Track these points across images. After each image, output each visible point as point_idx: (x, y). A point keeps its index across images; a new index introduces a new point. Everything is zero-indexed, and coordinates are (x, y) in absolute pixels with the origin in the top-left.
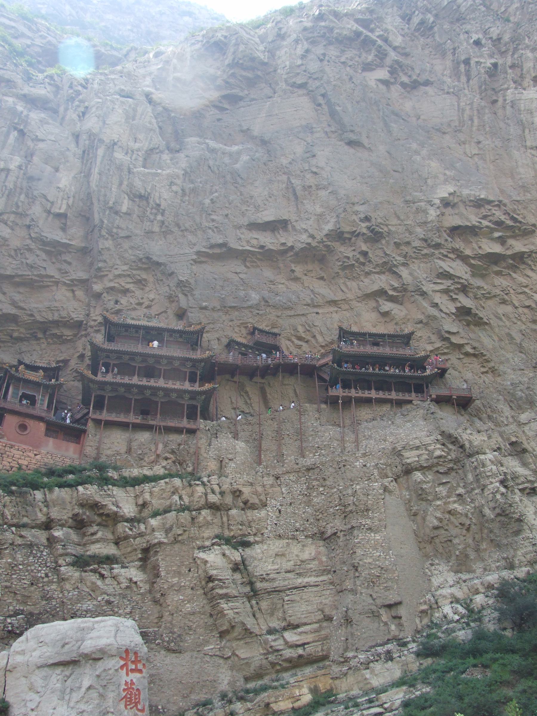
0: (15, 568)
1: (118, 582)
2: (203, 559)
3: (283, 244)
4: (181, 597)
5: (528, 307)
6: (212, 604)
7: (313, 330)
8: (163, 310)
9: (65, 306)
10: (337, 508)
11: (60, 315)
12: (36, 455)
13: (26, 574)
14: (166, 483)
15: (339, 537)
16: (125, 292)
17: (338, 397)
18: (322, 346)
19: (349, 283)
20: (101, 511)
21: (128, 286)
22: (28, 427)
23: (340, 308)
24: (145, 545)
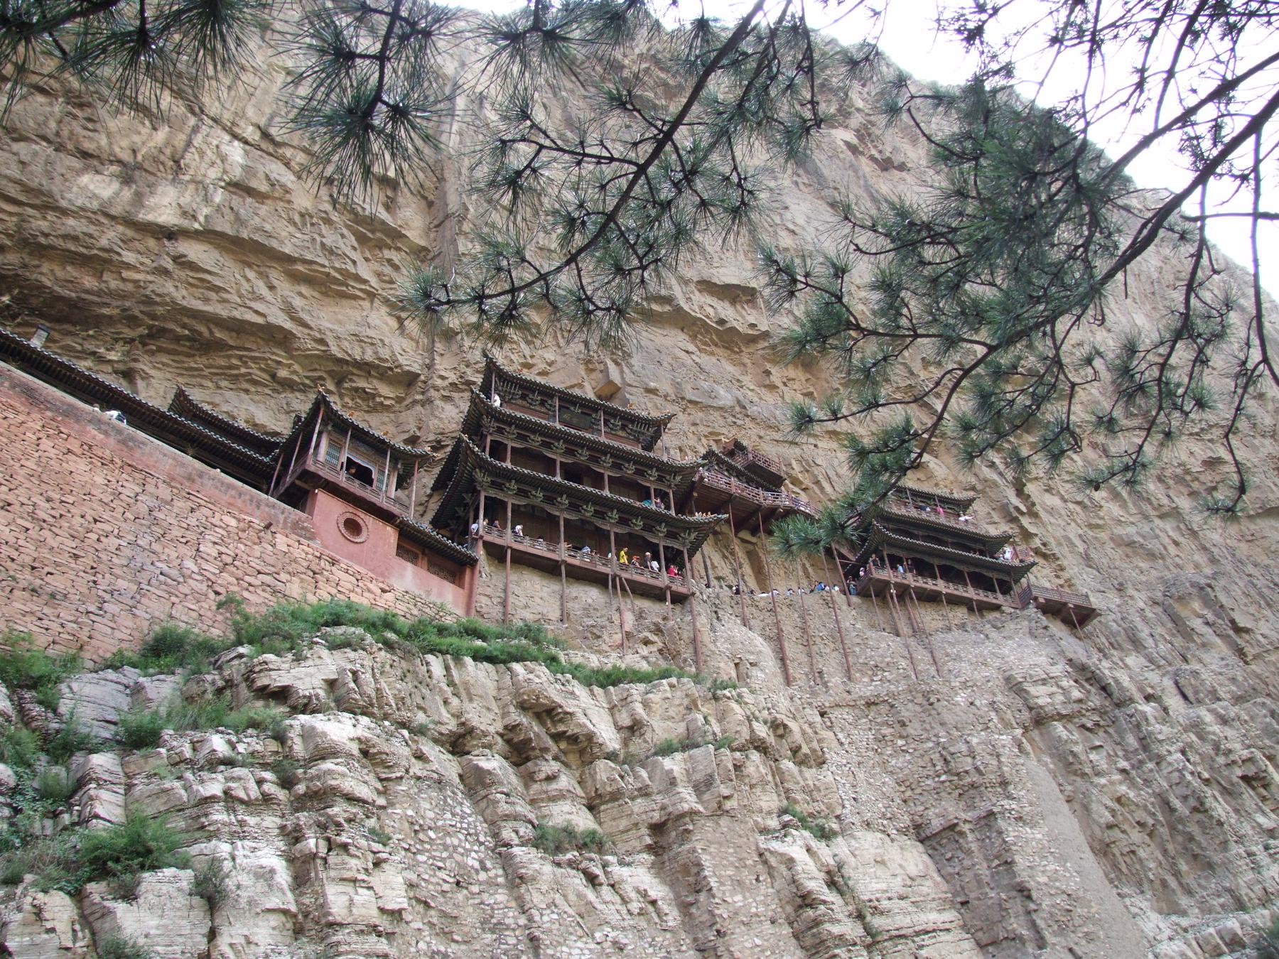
0: (421, 836)
1: (622, 898)
2: (782, 855)
3: (753, 326)
4: (758, 941)
5: (1078, 503)
7: (816, 471)
9: (387, 341)
10: (943, 778)
11: (376, 353)
12: (384, 591)
13: (445, 855)
14: (672, 686)
15: (962, 834)
18: (830, 500)
20: (561, 728)
22: (364, 529)
24: (656, 817)
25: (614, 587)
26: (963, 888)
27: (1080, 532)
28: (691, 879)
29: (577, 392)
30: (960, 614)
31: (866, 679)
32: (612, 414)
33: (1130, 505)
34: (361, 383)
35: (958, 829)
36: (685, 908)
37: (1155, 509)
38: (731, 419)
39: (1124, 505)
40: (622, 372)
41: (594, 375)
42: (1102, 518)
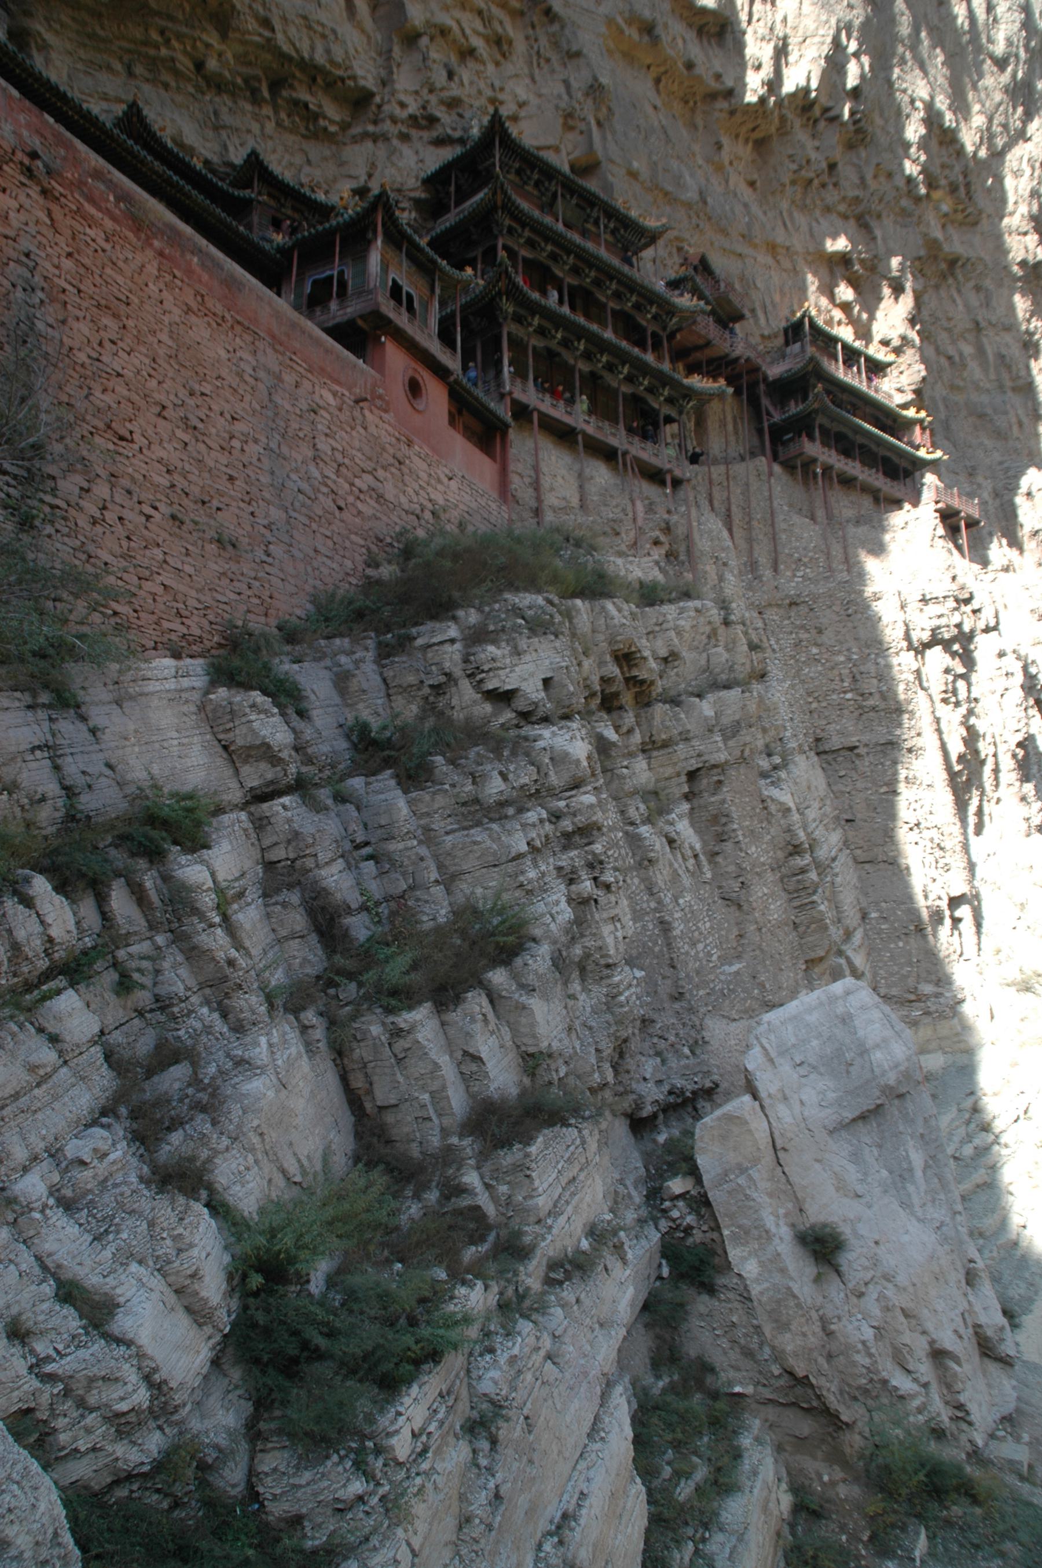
2: (781, 803)
3: (718, 77)
5: (950, 358)
6: (796, 903)
8: (550, 141)
10: (849, 696)
15: (858, 755)
16: (468, 53)
17: (814, 461)
19: (796, 214)
20: (635, 672)
21: (477, 42)
23: (778, 262)
24: (693, 764)
25: (625, 464)
26: (851, 807)
27: (944, 393)
28: (718, 828)
29: (550, 157)
30: (867, 502)
31: (788, 573)
32: (589, 201)
33: (992, 370)
34: (304, 95)
35: (856, 751)
36: (713, 855)
37: (1013, 380)
38: (694, 220)
39: (985, 369)
40: (604, 138)
41: (571, 136)
42: (964, 380)
